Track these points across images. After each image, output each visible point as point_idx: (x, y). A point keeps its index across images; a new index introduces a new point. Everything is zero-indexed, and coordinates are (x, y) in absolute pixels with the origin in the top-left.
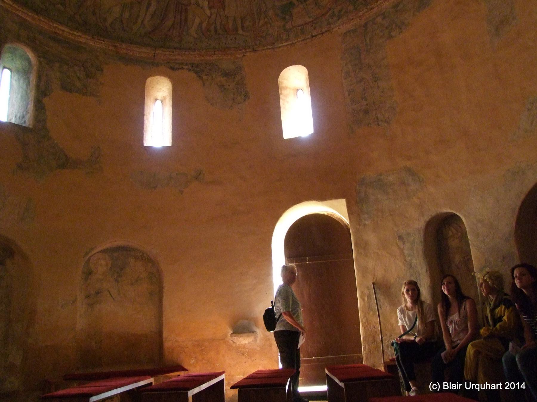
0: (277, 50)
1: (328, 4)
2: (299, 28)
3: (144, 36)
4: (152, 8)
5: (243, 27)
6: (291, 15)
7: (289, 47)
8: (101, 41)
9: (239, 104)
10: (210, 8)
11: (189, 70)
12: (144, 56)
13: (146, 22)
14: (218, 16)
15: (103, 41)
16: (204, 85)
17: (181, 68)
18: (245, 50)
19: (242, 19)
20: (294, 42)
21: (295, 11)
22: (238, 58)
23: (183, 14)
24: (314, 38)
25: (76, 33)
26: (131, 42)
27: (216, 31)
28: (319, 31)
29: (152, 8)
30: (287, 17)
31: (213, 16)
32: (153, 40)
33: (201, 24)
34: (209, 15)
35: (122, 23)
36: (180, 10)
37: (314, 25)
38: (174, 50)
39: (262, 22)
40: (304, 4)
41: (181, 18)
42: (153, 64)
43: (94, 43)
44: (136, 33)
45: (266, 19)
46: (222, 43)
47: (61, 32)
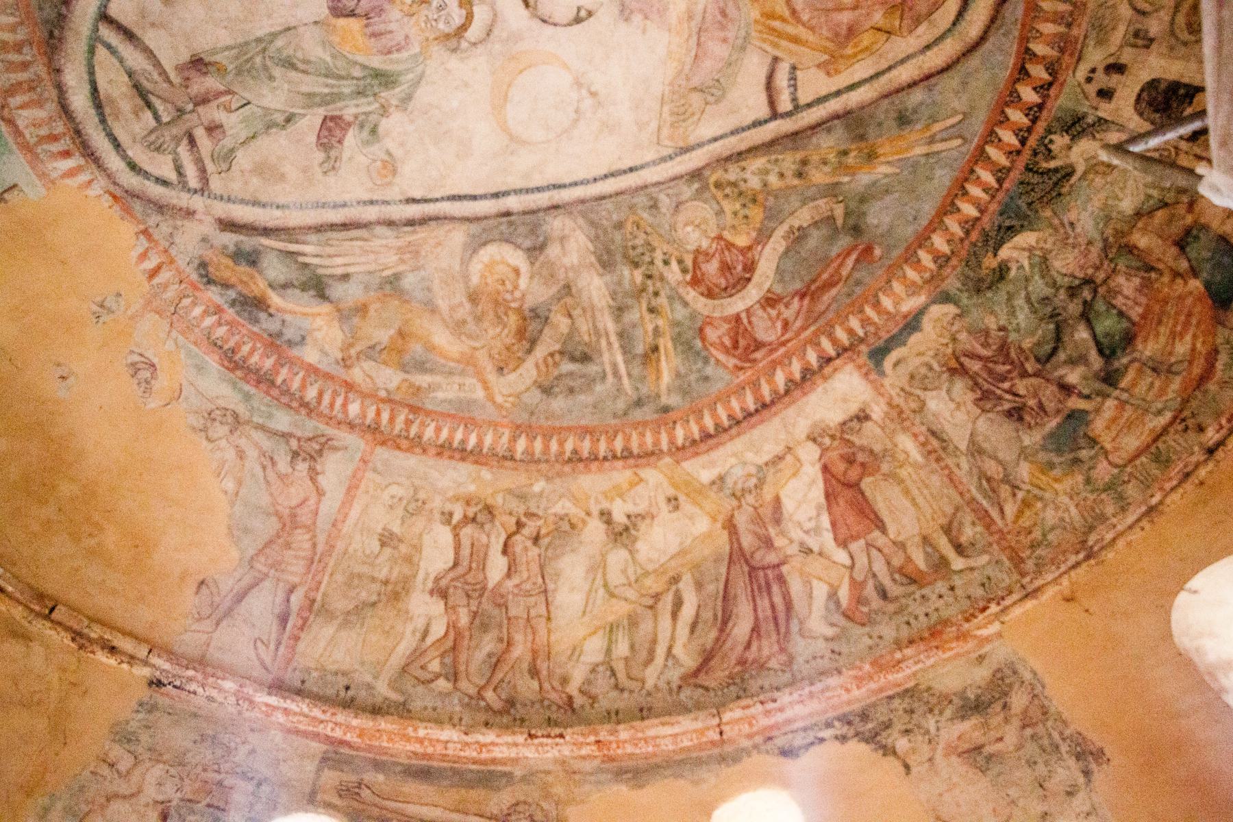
0: (1110, 555)
1: (1199, 345)
2: (1143, 459)
3: (680, 687)
4: (688, 612)
5: (959, 549)
6: (1093, 442)
7: (1144, 523)
8: (556, 736)
9: (1069, 794)
10: (843, 543)
11: (843, 739)
12: (689, 744)
13: (678, 650)
14: (874, 552)
15: (561, 736)
16: (907, 767)
17: (812, 744)
18: (998, 604)
19: (947, 530)
20: (1154, 501)
21: (1098, 426)
22: (988, 639)
23: (775, 589)
24: (1220, 454)
25: (481, 738)
26: (644, 713)
27: (884, 594)
28: (1224, 422)
29: (688, 612)
30: (1084, 454)
31: (862, 561)
32: (707, 689)
33: (833, 595)
34: (848, 562)
35: (613, 673)
36: (763, 583)
37: (1191, 426)
38: (776, 694)
39: (1010, 509)
40: (1116, 393)
41: (773, 607)
42: (722, 759)
43: (537, 751)
44: (656, 686)
45: (1020, 495)
46: (916, 618)
47: (439, 749)
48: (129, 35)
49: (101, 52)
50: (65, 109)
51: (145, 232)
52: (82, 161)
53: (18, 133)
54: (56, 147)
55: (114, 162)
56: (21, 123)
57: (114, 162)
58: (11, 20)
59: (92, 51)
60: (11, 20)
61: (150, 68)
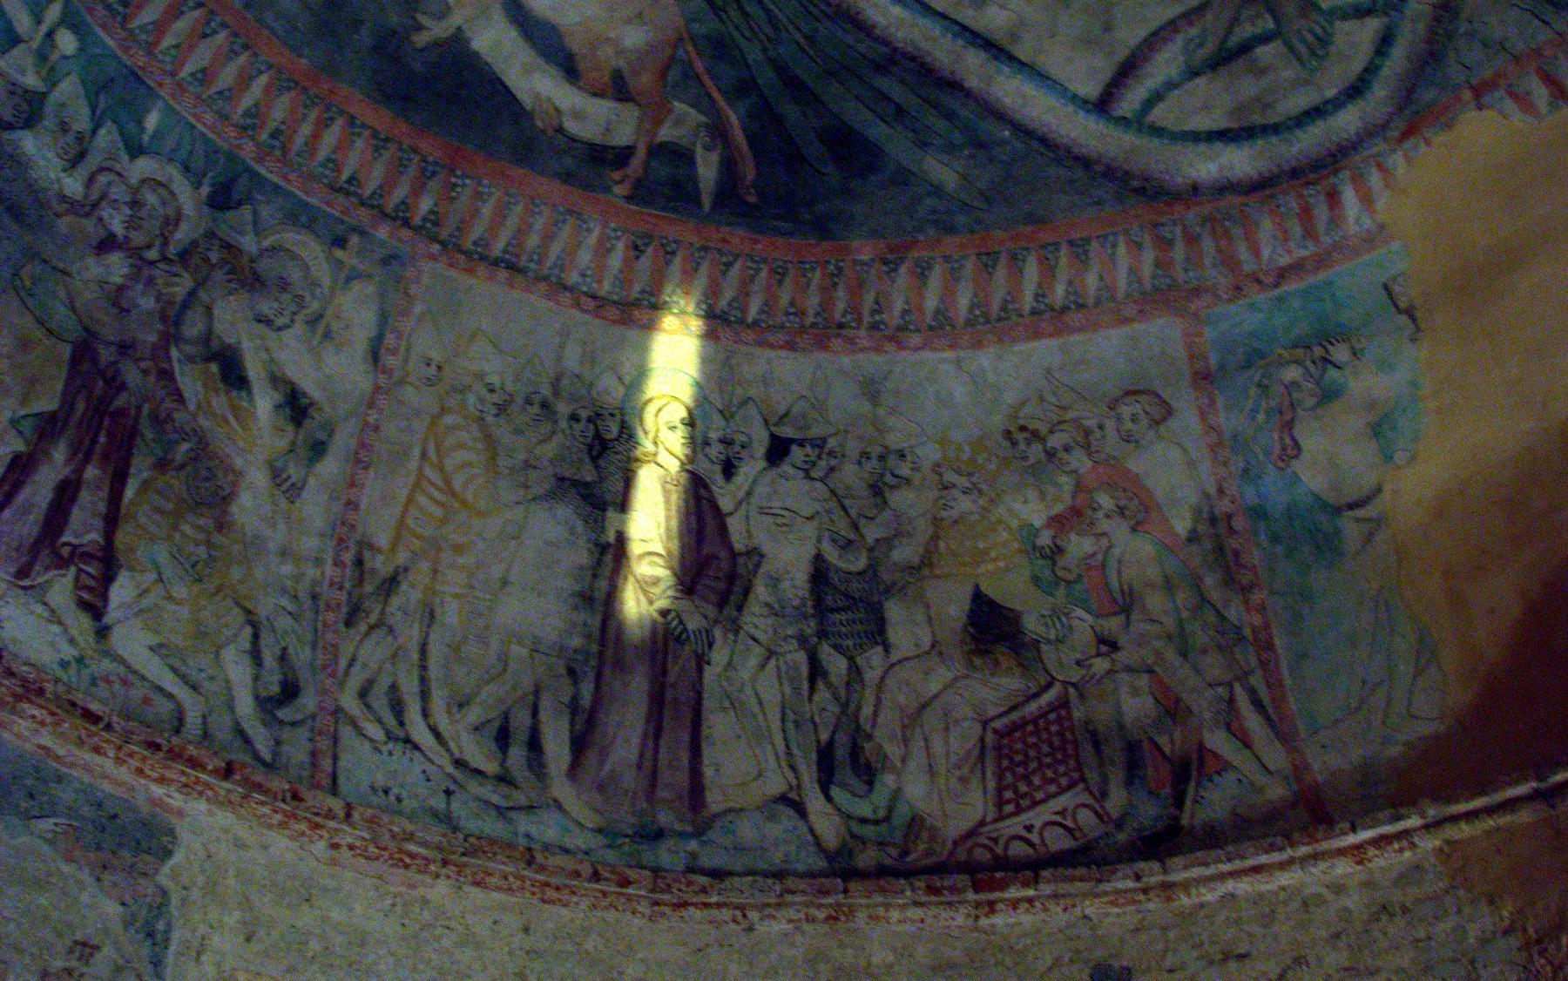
48: (1127, 70)
49: (1159, 114)
50: (1260, 186)
51: (1479, 91)
52: (1345, 175)
53: (1298, 267)
54: (1321, 212)
55: (1348, 121)
56: (1284, 260)
57: (1348, 121)
58: (1122, 249)
59: (1158, 131)
60: (1122, 249)
61: (1180, 40)
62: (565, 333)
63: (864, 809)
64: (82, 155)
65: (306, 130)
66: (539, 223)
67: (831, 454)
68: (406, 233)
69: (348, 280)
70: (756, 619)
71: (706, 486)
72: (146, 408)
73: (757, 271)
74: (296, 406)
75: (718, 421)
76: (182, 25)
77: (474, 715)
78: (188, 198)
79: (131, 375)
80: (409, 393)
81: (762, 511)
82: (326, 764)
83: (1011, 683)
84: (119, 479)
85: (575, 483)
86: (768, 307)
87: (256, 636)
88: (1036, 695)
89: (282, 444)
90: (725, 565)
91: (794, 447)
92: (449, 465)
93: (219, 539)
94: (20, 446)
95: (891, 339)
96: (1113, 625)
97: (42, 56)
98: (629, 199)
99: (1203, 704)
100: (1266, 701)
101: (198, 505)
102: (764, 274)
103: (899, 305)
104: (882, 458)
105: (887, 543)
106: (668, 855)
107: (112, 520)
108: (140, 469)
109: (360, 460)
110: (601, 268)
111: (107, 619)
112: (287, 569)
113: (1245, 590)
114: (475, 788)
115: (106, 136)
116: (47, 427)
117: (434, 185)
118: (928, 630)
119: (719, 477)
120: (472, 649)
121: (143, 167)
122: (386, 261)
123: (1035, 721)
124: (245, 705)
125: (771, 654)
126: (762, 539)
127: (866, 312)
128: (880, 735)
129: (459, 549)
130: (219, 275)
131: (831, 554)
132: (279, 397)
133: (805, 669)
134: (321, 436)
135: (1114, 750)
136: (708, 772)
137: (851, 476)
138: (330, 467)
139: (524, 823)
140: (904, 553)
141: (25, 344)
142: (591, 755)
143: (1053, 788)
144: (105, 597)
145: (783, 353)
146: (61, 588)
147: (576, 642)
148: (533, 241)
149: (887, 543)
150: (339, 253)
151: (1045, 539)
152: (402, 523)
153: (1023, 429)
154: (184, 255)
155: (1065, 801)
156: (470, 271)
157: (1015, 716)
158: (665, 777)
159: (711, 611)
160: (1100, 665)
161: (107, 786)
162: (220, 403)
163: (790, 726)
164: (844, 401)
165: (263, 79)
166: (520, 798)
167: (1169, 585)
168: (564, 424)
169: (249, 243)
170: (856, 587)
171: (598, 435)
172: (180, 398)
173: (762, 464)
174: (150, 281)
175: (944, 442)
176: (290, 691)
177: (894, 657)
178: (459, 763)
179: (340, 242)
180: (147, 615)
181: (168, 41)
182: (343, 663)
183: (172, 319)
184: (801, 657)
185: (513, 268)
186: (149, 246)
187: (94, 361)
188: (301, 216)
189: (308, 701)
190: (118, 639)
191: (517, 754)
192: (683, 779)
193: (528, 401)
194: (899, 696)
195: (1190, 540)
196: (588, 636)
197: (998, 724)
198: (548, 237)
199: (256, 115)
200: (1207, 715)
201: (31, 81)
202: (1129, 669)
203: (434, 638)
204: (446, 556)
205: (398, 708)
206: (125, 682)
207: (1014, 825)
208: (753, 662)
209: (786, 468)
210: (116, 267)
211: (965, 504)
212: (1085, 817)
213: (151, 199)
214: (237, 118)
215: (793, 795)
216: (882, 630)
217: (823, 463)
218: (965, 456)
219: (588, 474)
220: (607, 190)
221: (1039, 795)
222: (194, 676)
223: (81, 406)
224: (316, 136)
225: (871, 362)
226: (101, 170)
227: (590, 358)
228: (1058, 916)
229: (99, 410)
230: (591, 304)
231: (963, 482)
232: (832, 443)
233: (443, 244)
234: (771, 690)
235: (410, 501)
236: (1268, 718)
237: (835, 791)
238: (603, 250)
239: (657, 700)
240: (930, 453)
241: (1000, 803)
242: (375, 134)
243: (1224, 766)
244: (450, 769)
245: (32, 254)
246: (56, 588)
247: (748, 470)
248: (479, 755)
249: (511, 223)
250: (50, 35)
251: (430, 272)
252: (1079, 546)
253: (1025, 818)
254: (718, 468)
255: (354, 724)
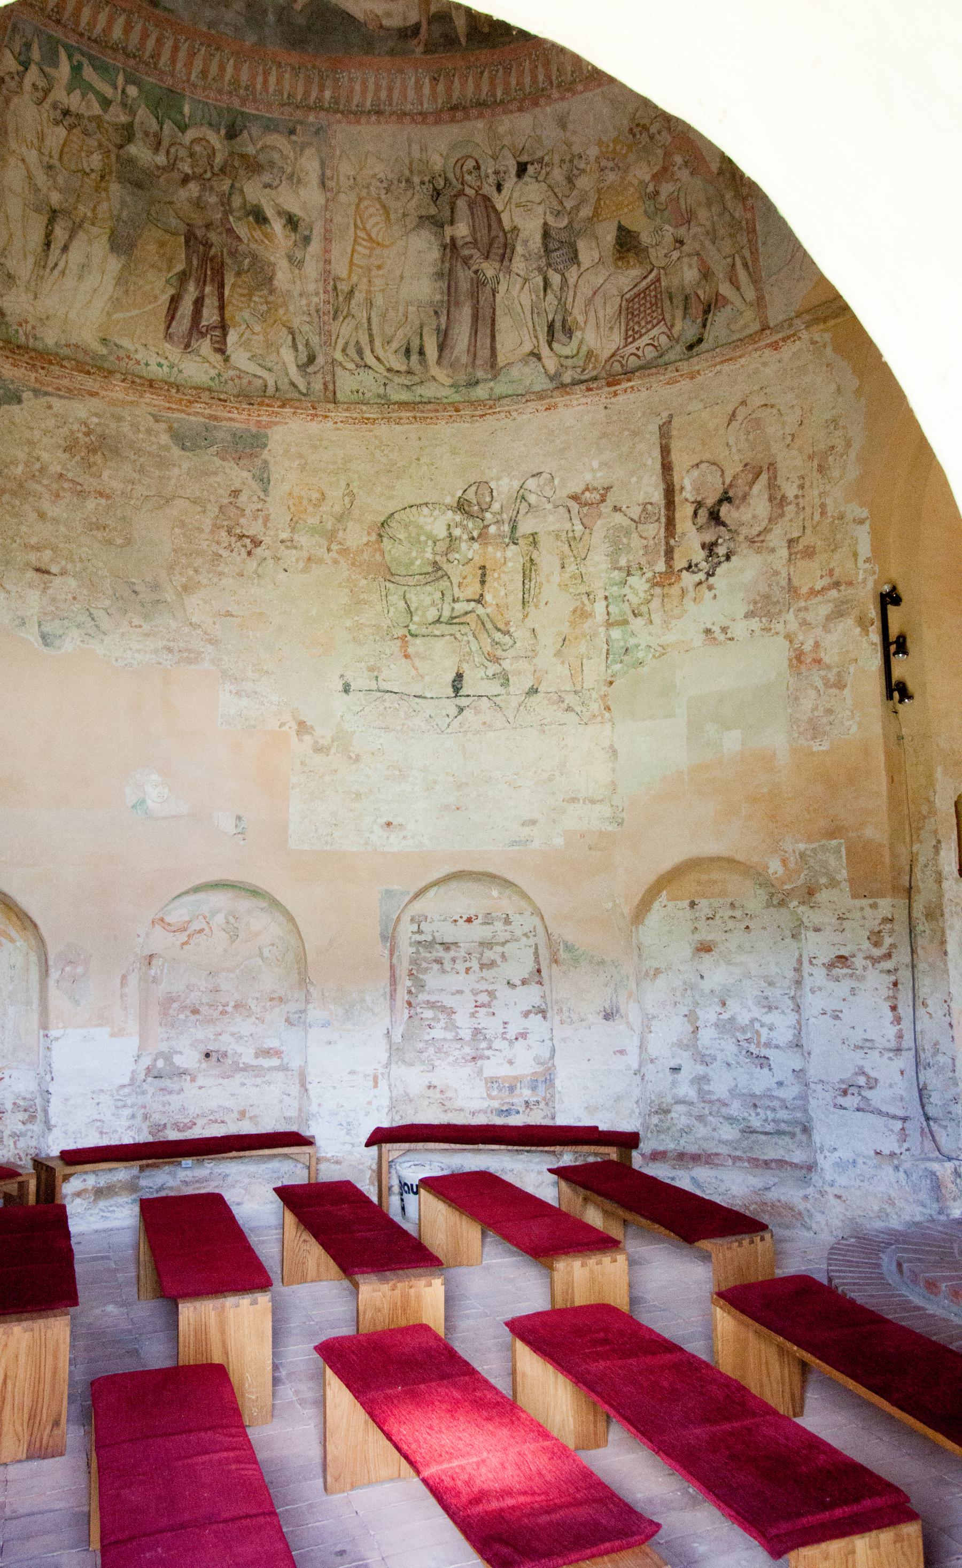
62: (410, 141)
63: (567, 351)
64: (159, 143)
65: (260, 79)
66: (384, 83)
67: (547, 165)
68: (322, 114)
69: (302, 151)
70: (518, 265)
71: (489, 200)
72: (225, 250)
73: (497, 71)
74: (292, 222)
75: (491, 162)
76: (182, 55)
77: (395, 345)
78: (215, 140)
79: (214, 237)
80: (343, 198)
81: (518, 206)
82: (331, 387)
83: (635, 273)
84: (222, 286)
85: (428, 218)
86: (506, 91)
87: (294, 339)
88: (645, 278)
89: (290, 243)
90: (502, 240)
91: (529, 167)
92: (368, 227)
93: (271, 298)
94: (172, 291)
95: (569, 90)
96: (682, 231)
97: (124, 105)
98: (425, 52)
99: (719, 268)
100: (750, 264)
101: (259, 286)
102: (501, 71)
103: (569, 69)
104: (571, 161)
105: (577, 208)
106: (481, 392)
107: (222, 308)
108: (229, 279)
109: (327, 239)
110: (420, 97)
111: (228, 353)
112: (304, 302)
113: (744, 199)
114: (398, 380)
115: (168, 127)
116: (183, 277)
117: (329, 83)
118: (597, 251)
119: (495, 193)
120: (392, 314)
121: (191, 134)
122: (317, 132)
123: (644, 291)
124: (293, 370)
125: (526, 280)
126: (518, 222)
127: (554, 78)
128: (576, 312)
129: (379, 267)
130: (242, 172)
131: (551, 220)
132: (283, 221)
133: (542, 284)
134: (307, 233)
135: (679, 300)
136: (498, 346)
137: (558, 174)
138: (315, 246)
139: (419, 390)
140: (585, 212)
141: (162, 244)
142: (447, 352)
143: (649, 326)
144: (225, 343)
145: (517, 114)
146: (205, 346)
147: (438, 297)
148: (383, 94)
149: (577, 208)
150: (294, 138)
151: (651, 188)
152: (351, 263)
153: (638, 125)
154: (223, 170)
155: (655, 332)
156: (358, 122)
157: (635, 290)
158: (480, 353)
159: (497, 265)
160: (675, 255)
161: (237, 425)
162: (258, 234)
163: (535, 316)
164: (551, 134)
165: (232, 62)
166: (416, 379)
167: (709, 205)
168: (418, 188)
169: (251, 150)
170: (564, 236)
171: (435, 189)
172: (238, 238)
173: (515, 179)
174: (212, 188)
175: (600, 143)
176: (312, 359)
177: (582, 269)
178: (389, 370)
179: (292, 132)
180: (246, 345)
181: (179, 65)
182: (334, 338)
183: (226, 201)
184: (539, 280)
185: (379, 113)
186: (205, 172)
187: (196, 238)
188: (270, 127)
189: (320, 360)
190: (233, 359)
191: (415, 358)
192: (487, 352)
193: (399, 181)
194: (585, 290)
195: (719, 174)
196: (442, 293)
197: (628, 296)
198: (390, 89)
199: (235, 81)
200: (721, 276)
201: (124, 119)
202: (689, 255)
203: (373, 314)
204: (374, 272)
205: (360, 352)
206: (240, 378)
207: (631, 348)
208: (518, 287)
209: (526, 179)
210: (194, 188)
211: (611, 177)
212: (664, 339)
213: (197, 148)
214: (226, 88)
215: (536, 351)
216: (576, 256)
217: (544, 172)
218: (610, 149)
219: (433, 211)
220: (413, 51)
221: (643, 331)
222: (270, 365)
223: (195, 262)
224: (265, 82)
225: (561, 106)
226: (170, 146)
227: (424, 149)
228: (644, 394)
229: (205, 259)
230: (420, 119)
231: (610, 164)
232: (546, 159)
233: (342, 113)
234: (526, 299)
235: (353, 251)
236: (750, 274)
237: (555, 345)
238: (419, 87)
239: (475, 317)
240: (593, 152)
241: (626, 339)
242: (293, 68)
243: (726, 301)
244: (385, 374)
245: (152, 202)
246: (203, 347)
247: (507, 186)
248: (398, 363)
249: (371, 87)
250: (123, 92)
251: (342, 132)
252: (667, 189)
253: (636, 344)
254: (494, 188)
255: (341, 364)
